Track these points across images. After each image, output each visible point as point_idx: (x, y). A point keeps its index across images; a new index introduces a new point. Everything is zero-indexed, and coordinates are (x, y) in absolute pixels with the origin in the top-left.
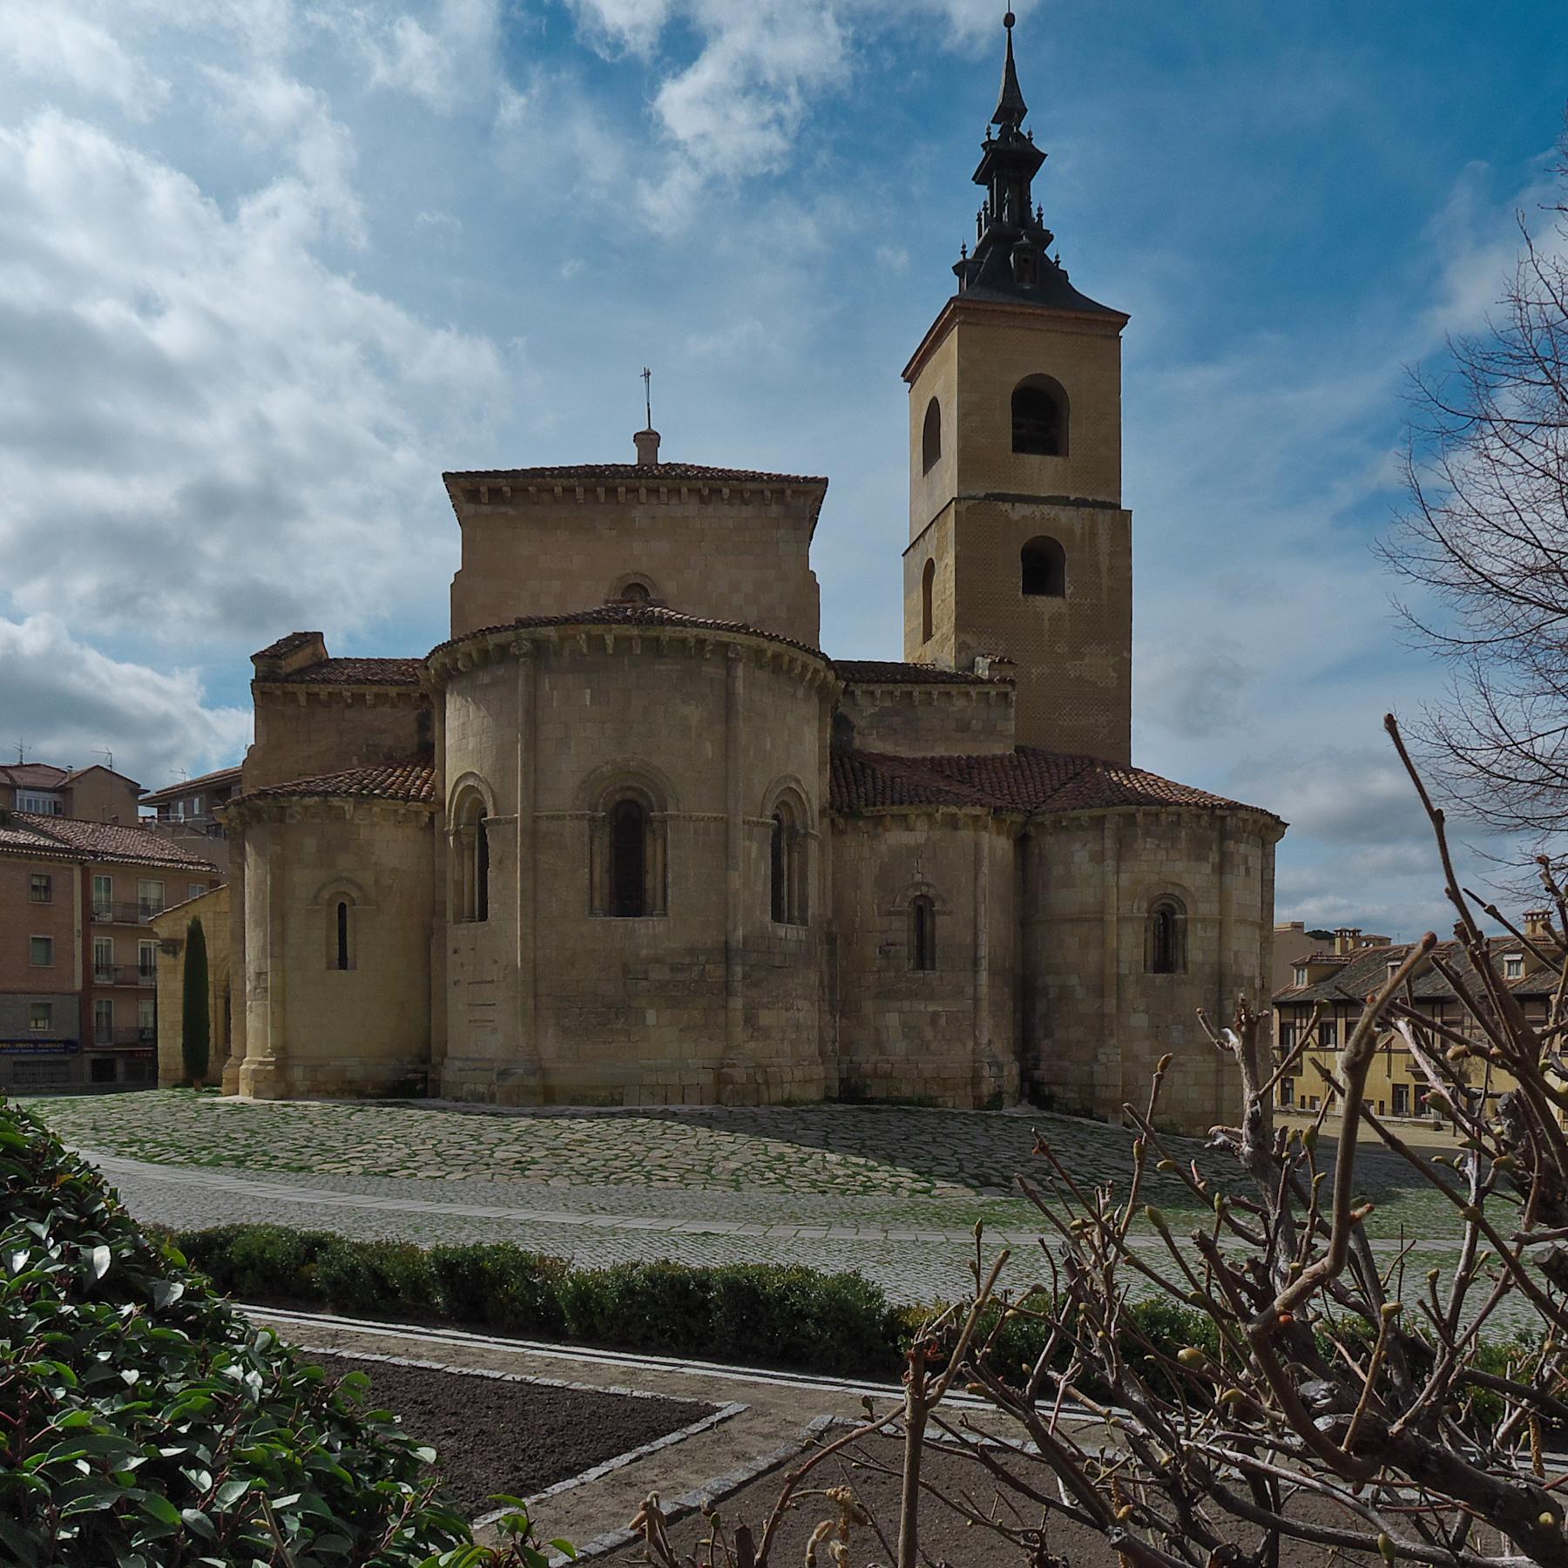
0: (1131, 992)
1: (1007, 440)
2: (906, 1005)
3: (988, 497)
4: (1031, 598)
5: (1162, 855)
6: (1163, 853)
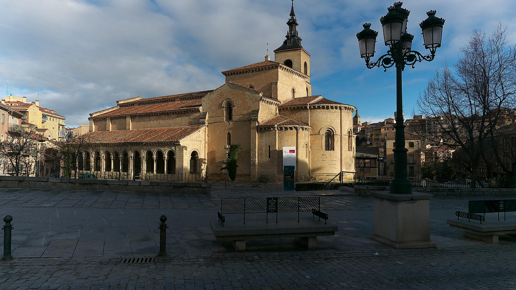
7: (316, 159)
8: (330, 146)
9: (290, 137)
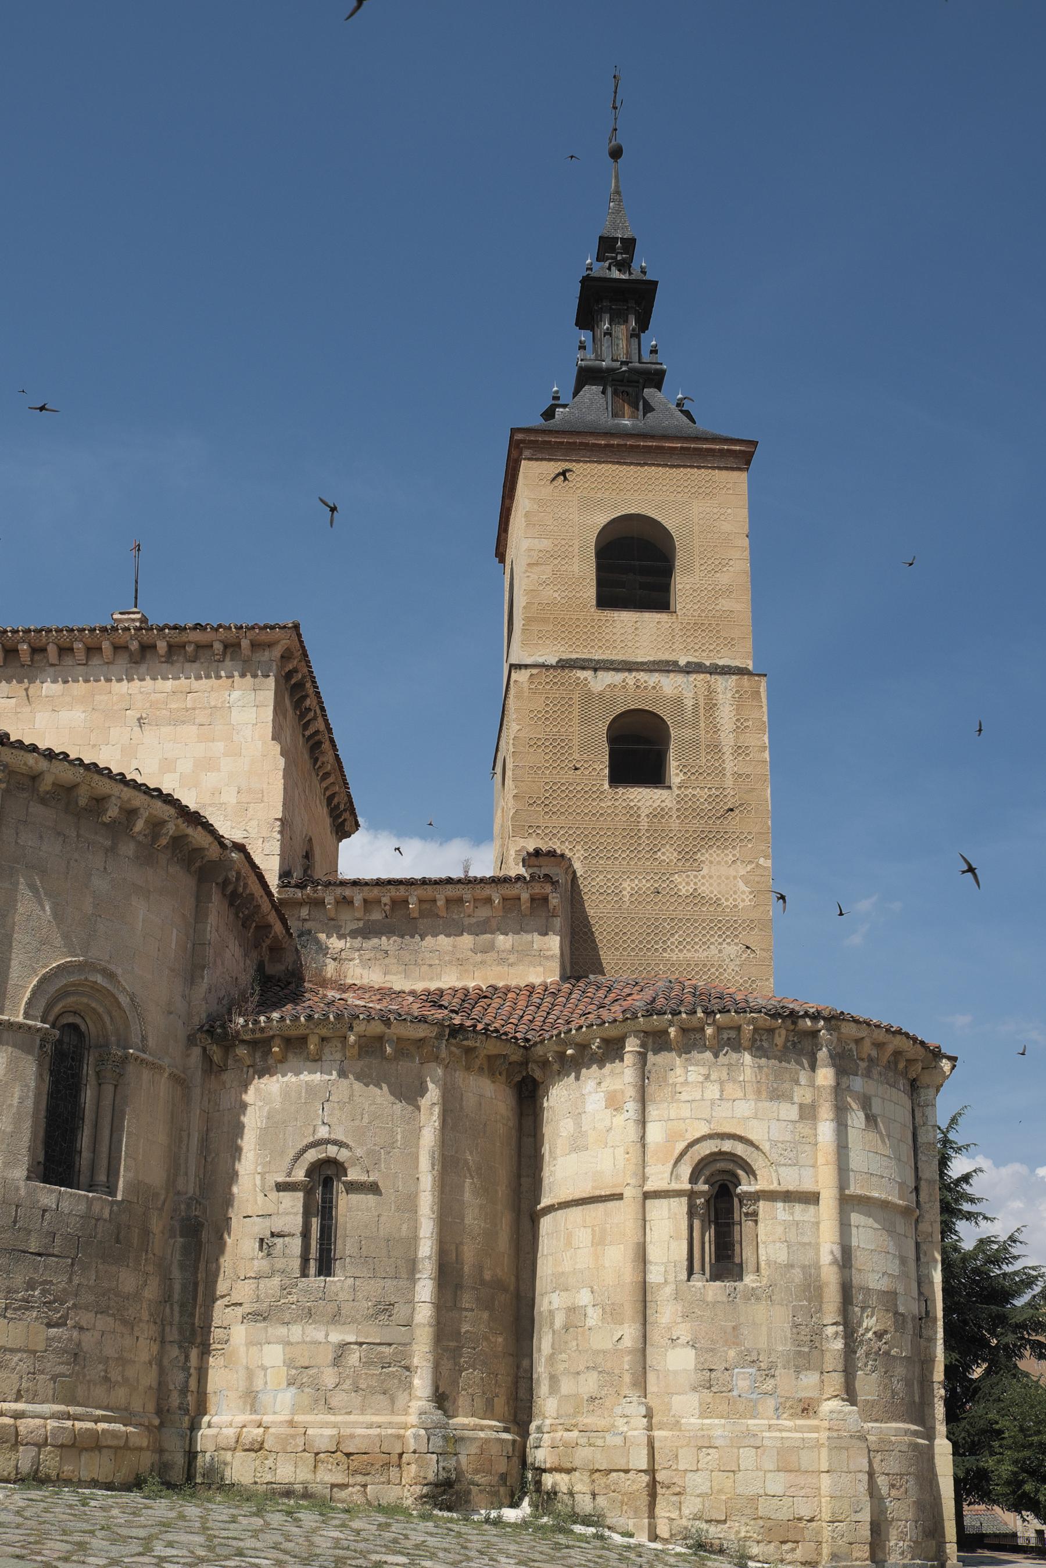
0: (666, 1313)
1: (590, 592)
2: (296, 1332)
3: (564, 665)
4: (621, 790)
5: (713, 1091)
6: (716, 1088)
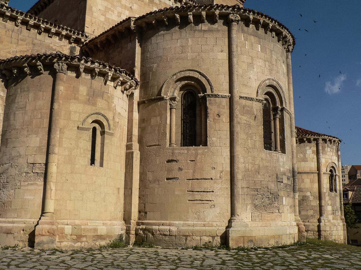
0: (327, 198)
7: (150, 176)
8: (194, 133)
9: (31, 95)
